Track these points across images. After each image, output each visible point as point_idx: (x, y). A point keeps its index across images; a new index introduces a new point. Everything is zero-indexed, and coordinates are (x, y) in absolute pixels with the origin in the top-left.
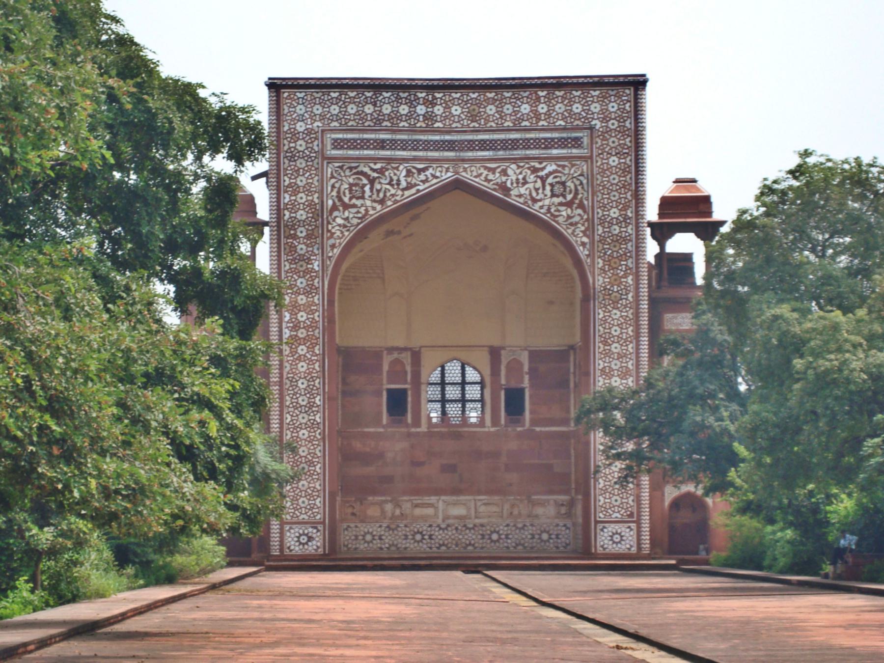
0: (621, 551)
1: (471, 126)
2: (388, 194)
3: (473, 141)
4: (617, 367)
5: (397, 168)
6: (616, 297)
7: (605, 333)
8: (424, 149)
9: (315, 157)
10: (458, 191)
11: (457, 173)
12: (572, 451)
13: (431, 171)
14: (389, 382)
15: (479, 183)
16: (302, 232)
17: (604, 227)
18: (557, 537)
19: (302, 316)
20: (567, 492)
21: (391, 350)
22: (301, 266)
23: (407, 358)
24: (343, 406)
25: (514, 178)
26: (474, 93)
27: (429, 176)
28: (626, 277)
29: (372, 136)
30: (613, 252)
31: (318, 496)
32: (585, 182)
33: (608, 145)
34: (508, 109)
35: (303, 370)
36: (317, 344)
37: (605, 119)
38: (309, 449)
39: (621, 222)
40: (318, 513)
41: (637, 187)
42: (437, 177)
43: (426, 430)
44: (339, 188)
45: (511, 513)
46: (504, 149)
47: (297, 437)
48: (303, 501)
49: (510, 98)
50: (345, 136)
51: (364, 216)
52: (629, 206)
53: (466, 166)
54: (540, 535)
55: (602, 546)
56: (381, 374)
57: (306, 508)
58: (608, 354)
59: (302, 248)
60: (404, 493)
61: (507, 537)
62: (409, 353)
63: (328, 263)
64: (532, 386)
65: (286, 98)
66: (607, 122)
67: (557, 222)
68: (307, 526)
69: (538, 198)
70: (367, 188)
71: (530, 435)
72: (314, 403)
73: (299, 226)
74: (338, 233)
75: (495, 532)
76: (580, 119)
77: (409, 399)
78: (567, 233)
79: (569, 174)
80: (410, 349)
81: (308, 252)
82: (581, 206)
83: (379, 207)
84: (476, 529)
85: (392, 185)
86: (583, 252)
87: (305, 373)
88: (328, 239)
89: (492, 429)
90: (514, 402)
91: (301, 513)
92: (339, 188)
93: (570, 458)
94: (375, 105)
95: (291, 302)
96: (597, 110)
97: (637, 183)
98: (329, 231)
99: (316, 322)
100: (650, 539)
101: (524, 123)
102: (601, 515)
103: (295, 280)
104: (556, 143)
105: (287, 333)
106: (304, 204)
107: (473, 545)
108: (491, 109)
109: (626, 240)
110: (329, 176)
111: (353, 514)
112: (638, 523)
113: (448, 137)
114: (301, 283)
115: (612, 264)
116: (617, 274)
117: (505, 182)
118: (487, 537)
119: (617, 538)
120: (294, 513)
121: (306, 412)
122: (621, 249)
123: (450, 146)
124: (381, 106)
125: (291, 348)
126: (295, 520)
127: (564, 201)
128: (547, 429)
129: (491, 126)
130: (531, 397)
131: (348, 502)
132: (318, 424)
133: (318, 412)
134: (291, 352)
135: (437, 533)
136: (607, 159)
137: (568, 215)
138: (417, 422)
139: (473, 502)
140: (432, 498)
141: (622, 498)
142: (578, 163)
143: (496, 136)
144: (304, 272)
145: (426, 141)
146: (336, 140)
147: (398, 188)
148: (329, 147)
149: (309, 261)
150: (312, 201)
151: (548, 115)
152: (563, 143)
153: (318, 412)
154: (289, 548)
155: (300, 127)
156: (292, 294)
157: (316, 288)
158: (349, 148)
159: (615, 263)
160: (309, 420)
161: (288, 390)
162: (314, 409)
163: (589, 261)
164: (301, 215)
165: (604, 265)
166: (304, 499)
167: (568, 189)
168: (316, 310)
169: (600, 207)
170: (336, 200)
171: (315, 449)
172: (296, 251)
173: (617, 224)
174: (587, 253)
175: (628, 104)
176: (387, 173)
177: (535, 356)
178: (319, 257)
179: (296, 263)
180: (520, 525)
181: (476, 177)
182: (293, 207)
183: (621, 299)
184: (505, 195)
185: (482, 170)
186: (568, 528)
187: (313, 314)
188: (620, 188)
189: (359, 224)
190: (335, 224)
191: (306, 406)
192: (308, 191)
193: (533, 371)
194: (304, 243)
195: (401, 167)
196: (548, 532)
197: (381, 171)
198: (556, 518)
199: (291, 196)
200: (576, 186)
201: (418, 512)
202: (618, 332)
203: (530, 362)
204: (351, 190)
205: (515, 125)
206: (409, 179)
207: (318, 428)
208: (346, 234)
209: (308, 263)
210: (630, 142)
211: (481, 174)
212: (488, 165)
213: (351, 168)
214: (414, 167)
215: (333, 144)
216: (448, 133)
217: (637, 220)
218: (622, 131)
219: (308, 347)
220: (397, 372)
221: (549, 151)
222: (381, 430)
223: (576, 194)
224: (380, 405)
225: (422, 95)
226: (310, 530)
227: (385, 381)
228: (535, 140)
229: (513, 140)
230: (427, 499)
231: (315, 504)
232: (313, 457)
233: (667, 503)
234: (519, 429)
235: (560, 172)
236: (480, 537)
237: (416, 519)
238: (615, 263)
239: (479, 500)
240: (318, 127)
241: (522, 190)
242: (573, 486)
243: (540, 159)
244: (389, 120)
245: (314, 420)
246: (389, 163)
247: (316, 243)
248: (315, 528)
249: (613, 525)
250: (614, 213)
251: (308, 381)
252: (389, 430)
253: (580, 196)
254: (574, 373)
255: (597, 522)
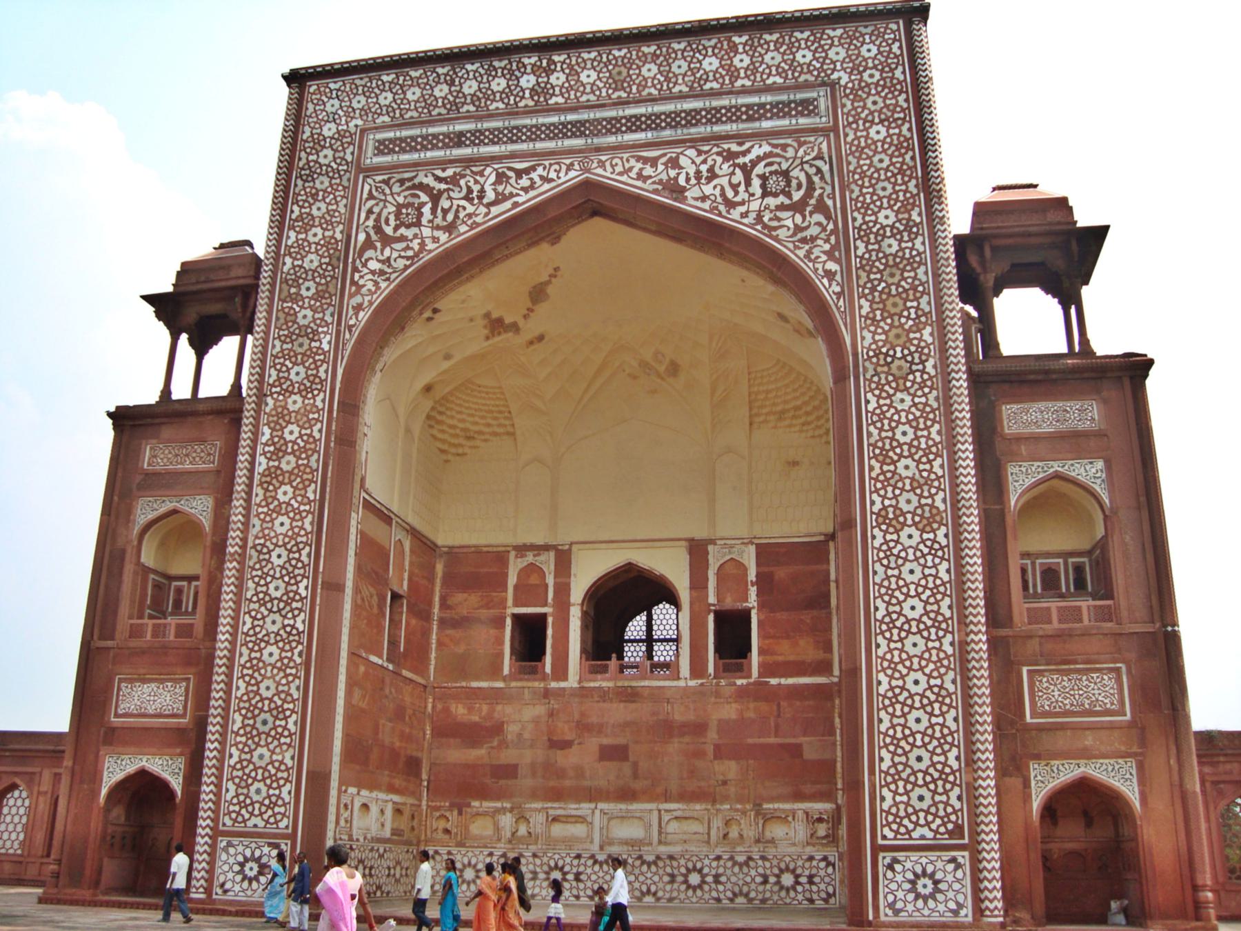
0: (935, 918)
1: (614, 96)
2: (462, 215)
3: (618, 119)
4: (911, 508)
5: (481, 174)
6: (900, 368)
7: (882, 439)
8: (530, 139)
9: (346, 171)
10: (598, 222)
11: (588, 171)
12: (837, 720)
13: (540, 170)
14: (516, 605)
15: (628, 183)
16: (308, 289)
17: (868, 243)
18: (811, 882)
19: (292, 432)
20: (828, 796)
21: (522, 549)
22: (301, 345)
23: (548, 562)
24: (440, 644)
25: (692, 171)
26: (620, 50)
27: (537, 179)
28: (919, 330)
29: (444, 129)
30: (888, 286)
31: (287, 780)
32: (825, 168)
33: (864, 107)
34: (679, 67)
35: (283, 530)
36: (311, 481)
37: (857, 68)
38: (279, 684)
39: (900, 232)
40: (284, 815)
41: (926, 172)
42: (552, 180)
43: (576, 685)
44: (379, 215)
45: (725, 836)
46: (672, 127)
47: (260, 660)
48: (258, 791)
49: (684, 51)
50: (398, 134)
51: (416, 255)
52: (914, 205)
53: (603, 158)
54: (778, 876)
55: (891, 906)
56: (506, 590)
57: (262, 804)
58: (891, 480)
59: (305, 316)
60: (534, 795)
61: (717, 878)
62: (552, 554)
63: (347, 336)
64: (762, 606)
65: (314, 93)
66: (860, 73)
67: (776, 239)
68: (261, 841)
69: (738, 199)
70: (426, 210)
71: (759, 692)
72: (296, 593)
73: (305, 279)
74: (370, 285)
75: (695, 869)
76: (810, 72)
77: (550, 632)
78: (797, 256)
79: (795, 158)
80: (554, 547)
81: (314, 320)
82: (821, 207)
83: (444, 237)
84: (661, 864)
85: (470, 200)
86: (829, 290)
87: (286, 535)
88: (351, 296)
89: (692, 683)
90: (732, 635)
91: (252, 814)
92: (379, 215)
93: (834, 734)
94: (452, 83)
95: (275, 408)
96: (841, 57)
97: (925, 165)
98: (353, 283)
99: (315, 441)
100: (1003, 888)
101: (708, 86)
102: (886, 831)
103: (288, 370)
104: (770, 111)
105: (262, 464)
106: (317, 244)
107: (655, 894)
108: (650, 70)
109: (913, 263)
110: (365, 196)
111: (447, 831)
112: (975, 850)
113: (571, 117)
114: (297, 374)
115: (889, 307)
116: (901, 325)
117: (676, 179)
118: (680, 879)
119: (924, 886)
120: (239, 813)
121: (279, 611)
122: (905, 279)
123: (578, 129)
124: (461, 85)
125: (267, 490)
126: (239, 828)
127: (787, 202)
128: (791, 681)
129: (650, 94)
130: (759, 621)
131: (437, 809)
132: (299, 633)
133: (300, 610)
134: (265, 499)
135: (589, 871)
136: (866, 129)
137: (796, 225)
138: (561, 671)
139: (656, 813)
140: (584, 805)
141: (935, 792)
142: (812, 139)
143: (658, 108)
144: (304, 354)
145: (532, 126)
146: (381, 142)
147: (481, 203)
148: (369, 154)
149: (314, 335)
150: (332, 237)
151: (752, 70)
152: (780, 110)
153: (300, 610)
154: (222, 885)
155: (329, 130)
156: (279, 393)
157: (321, 381)
158: (403, 151)
159: (895, 305)
160: (284, 627)
161: (253, 569)
162: (294, 605)
163: (841, 303)
164: (311, 261)
165: (873, 311)
166: (261, 785)
167: (794, 183)
168: (317, 420)
169: (858, 209)
170: (372, 233)
171: (288, 683)
172: (294, 322)
173: (893, 236)
174: (838, 289)
175: (897, 44)
176: (462, 182)
177: (766, 553)
178: (333, 329)
179: (292, 342)
180: (741, 859)
181: (620, 174)
182: (301, 249)
183: (913, 372)
184: (675, 200)
185: (633, 162)
186: (829, 864)
187: (311, 427)
188: (894, 175)
189: (406, 267)
190: (366, 271)
191: (280, 600)
192: (327, 223)
193: (764, 581)
194: (310, 307)
195: (489, 170)
196: (793, 871)
197: (454, 181)
198: (808, 844)
199: (298, 233)
200: (807, 173)
201: (558, 830)
202: (911, 435)
203: (758, 565)
204: (398, 214)
205: (691, 88)
206: (500, 188)
207: (299, 643)
208: (383, 285)
209: (312, 340)
210: (907, 100)
211: (631, 169)
212: (645, 154)
213: (402, 182)
214: (510, 169)
215: (376, 148)
216: (574, 109)
217: (932, 227)
218: (890, 86)
219: (295, 488)
220: (530, 588)
221: (757, 124)
222: (500, 684)
223: (811, 187)
224: (502, 643)
225: (530, 60)
226: (266, 850)
227: (510, 602)
228: (728, 109)
229: (688, 113)
230: (572, 808)
231: (279, 797)
232: (284, 701)
233: (1036, 804)
234: (739, 682)
235: (778, 155)
236: (666, 879)
237: (552, 843)
238: (895, 305)
239: (667, 811)
240: (356, 126)
241: (708, 190)
242: (840, 786)
243: (740, 138)
244: (473, 103)
245: (293, 627)
246: (468, 167)
247: (330, 305)
248: (276, 846)
249: (914, 856)
250: (887, 217)
251: (290, 551)
252: (514, 684)
253: (817, 193)
254: (837, 581)
255: (876, 849)
